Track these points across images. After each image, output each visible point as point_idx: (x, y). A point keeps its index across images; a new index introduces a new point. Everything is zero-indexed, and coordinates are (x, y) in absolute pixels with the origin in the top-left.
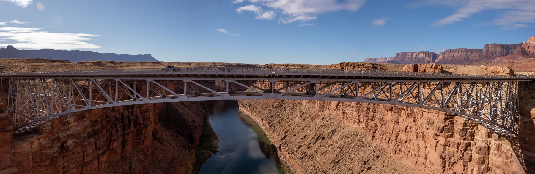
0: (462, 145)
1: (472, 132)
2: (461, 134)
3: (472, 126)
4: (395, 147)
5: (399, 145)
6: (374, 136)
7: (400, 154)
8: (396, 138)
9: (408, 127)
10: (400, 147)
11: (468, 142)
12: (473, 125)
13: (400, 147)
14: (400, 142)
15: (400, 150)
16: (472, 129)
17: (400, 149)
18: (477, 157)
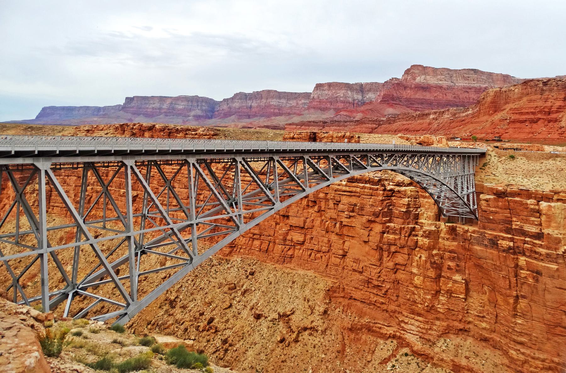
0: (405, 230)
1: (415, 214)
2: (404, 217)
3: (415, 208)
4: (283, 253)
5: (289, 250)
6: (233, 246)
7: (293, 261)
8: (285, 240)
9: (308, 220)
10: (290, 253)
11: (413, 226)
12: (417, 206)
13: (290, 253)
14: (291, 245)
15: (292, 257)
16: (416, 211)
17: (291, 255)
18: (426, 241)
